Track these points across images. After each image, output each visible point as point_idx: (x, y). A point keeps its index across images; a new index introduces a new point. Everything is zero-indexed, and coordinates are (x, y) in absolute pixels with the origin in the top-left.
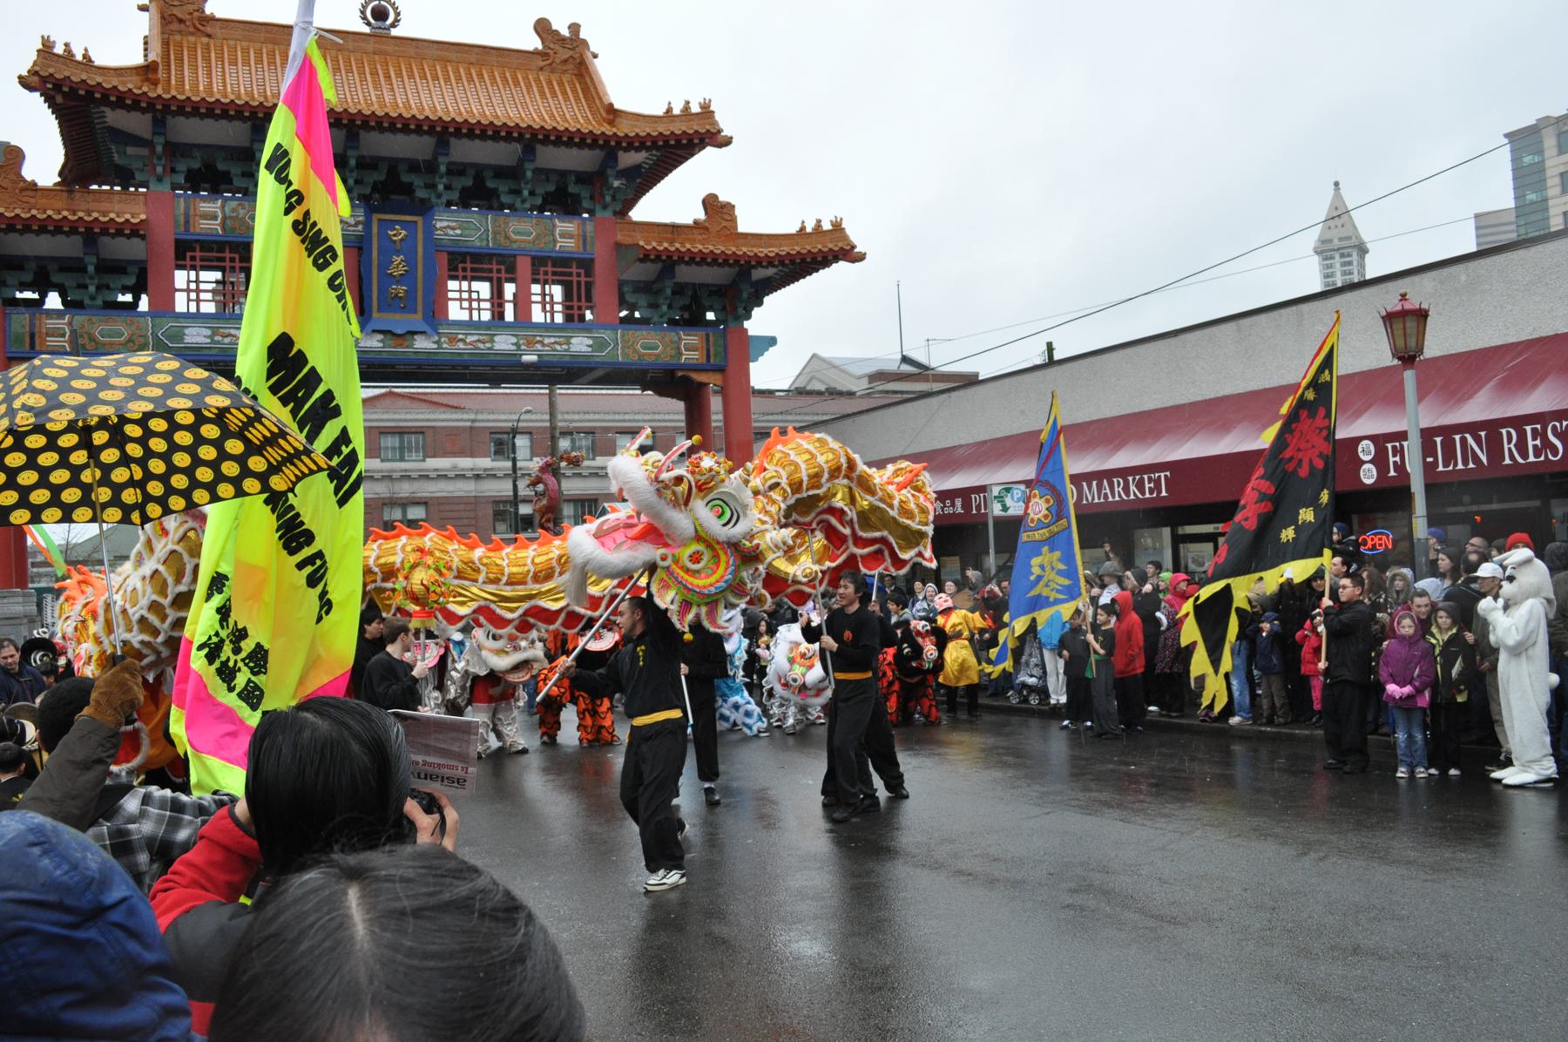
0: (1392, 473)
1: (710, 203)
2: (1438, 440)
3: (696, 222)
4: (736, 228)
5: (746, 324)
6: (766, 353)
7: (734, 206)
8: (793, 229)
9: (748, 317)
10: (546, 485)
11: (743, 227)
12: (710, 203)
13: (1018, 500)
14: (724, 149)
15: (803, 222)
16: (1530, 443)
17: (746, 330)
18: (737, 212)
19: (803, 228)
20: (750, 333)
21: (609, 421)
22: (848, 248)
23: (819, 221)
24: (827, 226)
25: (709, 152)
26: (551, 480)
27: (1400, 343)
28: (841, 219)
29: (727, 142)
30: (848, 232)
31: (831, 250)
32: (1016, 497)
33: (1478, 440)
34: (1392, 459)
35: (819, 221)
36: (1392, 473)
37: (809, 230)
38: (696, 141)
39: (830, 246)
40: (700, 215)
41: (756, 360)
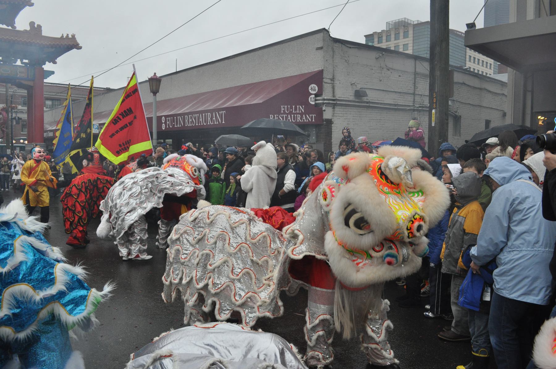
0: (167, 127)
1: (32, 24)
2: (175, 117)
3: (26, 30)
4: (41, 34)
5: (43, 66)
6: (50, 77)
7: (41, 27)
8: (59, 36)
9: (45, 64)
10: (3, 115)
11: (44, 33)
12: (32, 24)
13: (96, 129)
14: (31, 7)
15: (63, 34)
16: (190, 120)
17: (43, 68)
18: (43, 29)
19: (63, 36)
20: (44, 69)
21: (63, 96)
22: (76, 44)
23: (68, 35)
24: (70, 36)
25: (27, 7)
26: (4, 113)
27: (151, 87)
28: (75, 35)
29: (32, 5)
30: (77, 39)
31: (69, 44)
32: (95, 128)
33: (181, 118)
34: (168, 123)
35: (68, 35)
36: (167, 127)
37: (64, 37)
38: (21, 3)
39: (69, 43)
40: (28, 28)
41: (46, 78)
